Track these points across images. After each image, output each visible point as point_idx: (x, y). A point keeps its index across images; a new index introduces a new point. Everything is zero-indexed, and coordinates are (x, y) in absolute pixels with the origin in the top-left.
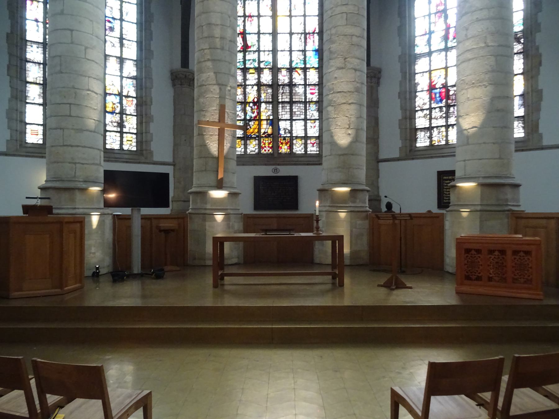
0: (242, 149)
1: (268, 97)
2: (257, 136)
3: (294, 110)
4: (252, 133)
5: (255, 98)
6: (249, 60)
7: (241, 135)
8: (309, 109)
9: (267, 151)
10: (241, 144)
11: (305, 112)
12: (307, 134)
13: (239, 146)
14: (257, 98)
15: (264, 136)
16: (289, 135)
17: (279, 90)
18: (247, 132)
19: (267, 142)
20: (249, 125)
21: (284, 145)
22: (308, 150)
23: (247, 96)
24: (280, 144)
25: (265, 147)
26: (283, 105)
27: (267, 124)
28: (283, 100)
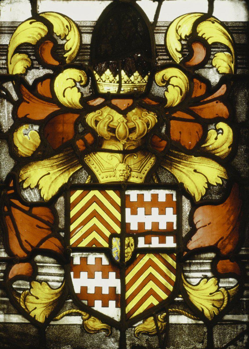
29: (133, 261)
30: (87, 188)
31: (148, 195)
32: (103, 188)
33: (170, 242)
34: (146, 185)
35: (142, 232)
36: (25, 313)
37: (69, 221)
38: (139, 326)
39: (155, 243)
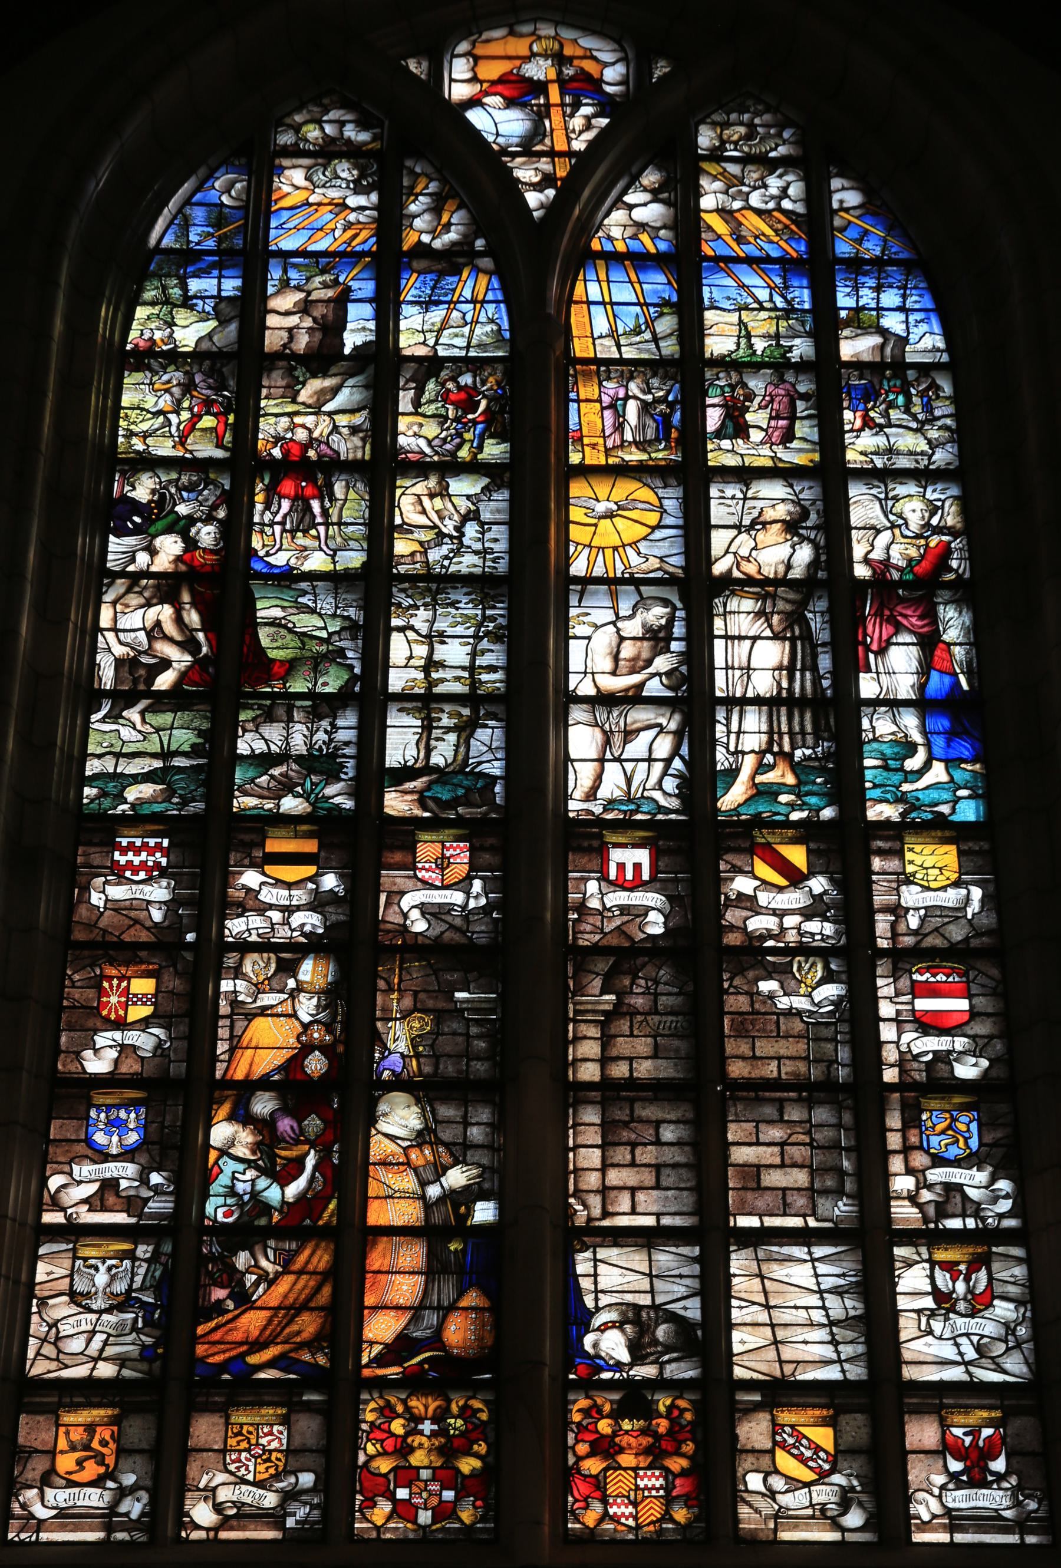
0: (122, 1493)
1: (446, 1044)
2: (312, 1377)
3: (741, 1155)
4: (257, 1345)
5: (306, 1049)
6: (265, 761)
7: (122, 1361)
8: (906, 1150)
9: (424, 1517)
10: (121, 1452)
11: (859, 1174)
12: (898, 1362)
13: (92, 1470)
14: (324, 1049)
15: (392, 1372)
16: (682, 1371)
17: (580, 990)
18: (195, 1340)
19: (427, 1427)
20: (232, 1278)
21: (627, 1460)
22: (925, 1507)
23: (223, 1033)
24: (583, 1448)
25: (406, 1475)
26: (621, 1115)
27: (433, 1270)
28: (620, 1070)
29: (642, 1501)
30: (615, 1469)
31: (649, 1473)
32: (625, 1469)
33: (662, 1492)
34: (649, 1468)
35: (646, 1488)
36: (583, 1524)
37: (606, 1484)
38: (646, 1529)
39: (654, 1493)
